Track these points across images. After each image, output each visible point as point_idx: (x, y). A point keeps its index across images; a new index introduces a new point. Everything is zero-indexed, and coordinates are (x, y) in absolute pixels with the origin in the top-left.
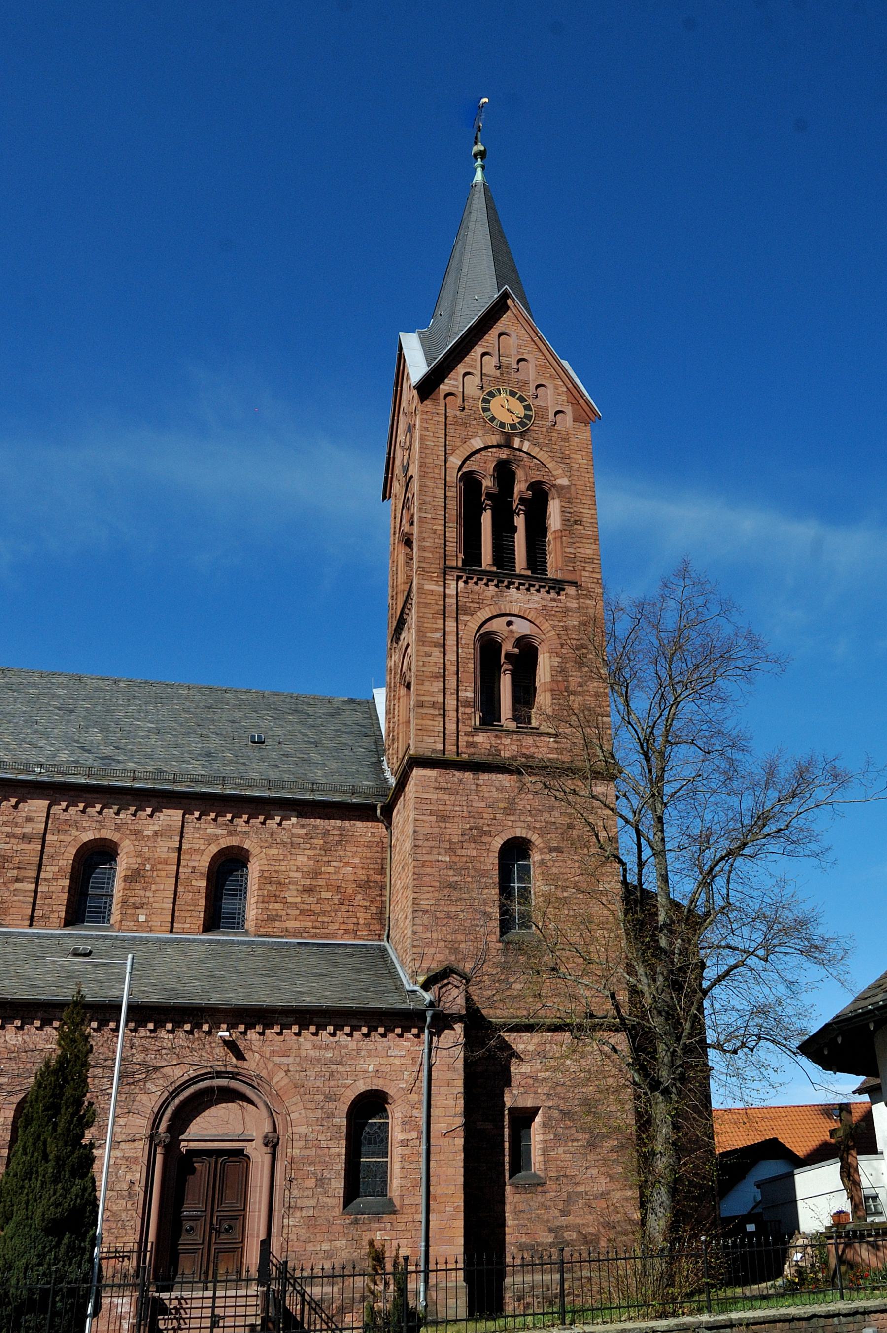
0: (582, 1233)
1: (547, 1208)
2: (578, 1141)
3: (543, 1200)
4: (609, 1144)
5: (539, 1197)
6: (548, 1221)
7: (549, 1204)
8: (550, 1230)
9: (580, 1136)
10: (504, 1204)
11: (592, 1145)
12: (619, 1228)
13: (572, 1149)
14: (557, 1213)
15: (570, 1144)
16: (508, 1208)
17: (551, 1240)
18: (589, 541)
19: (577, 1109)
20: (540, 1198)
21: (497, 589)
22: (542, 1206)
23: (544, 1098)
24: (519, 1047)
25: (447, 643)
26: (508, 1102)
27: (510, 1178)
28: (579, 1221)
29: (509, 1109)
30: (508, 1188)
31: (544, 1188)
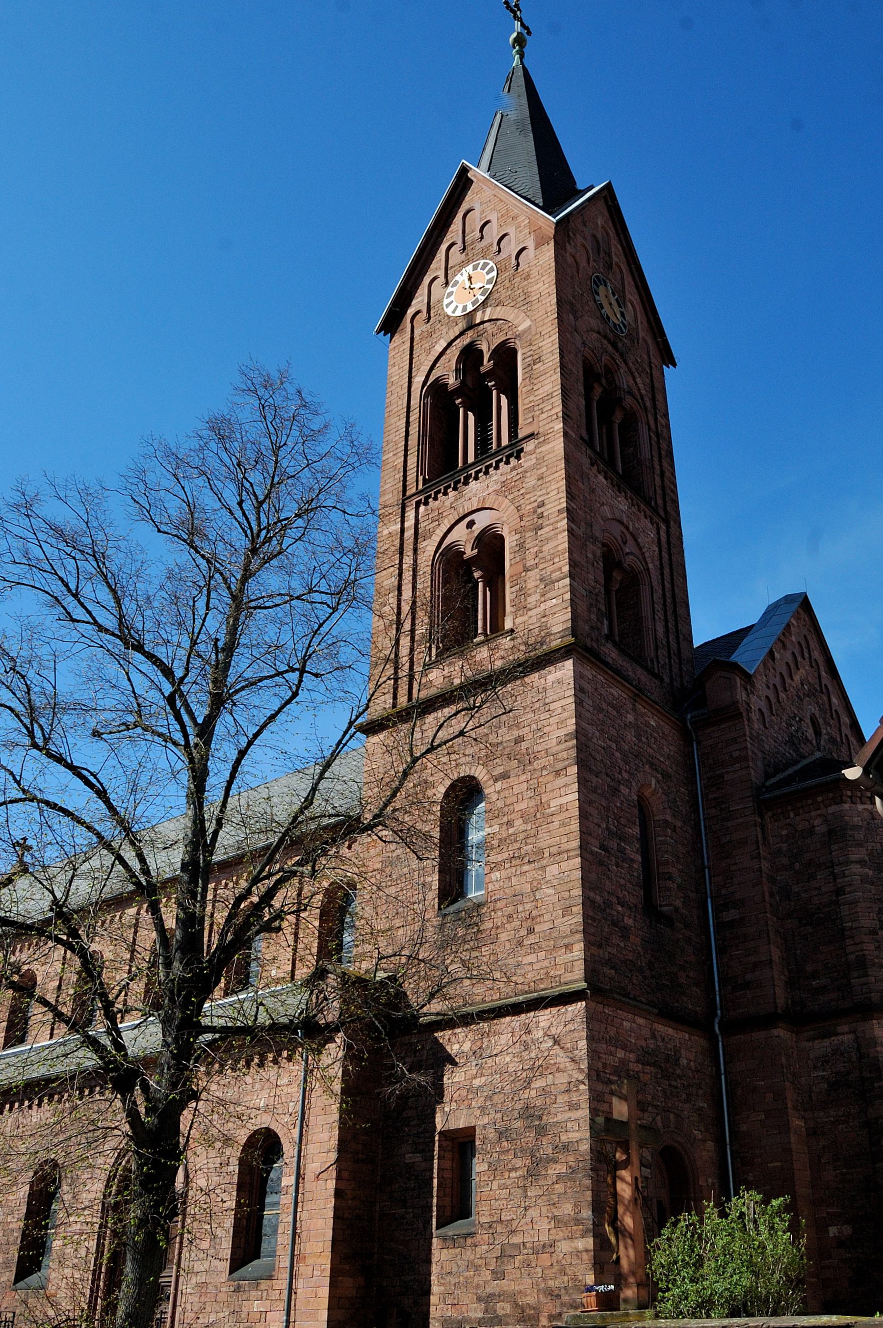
0: (517, 1305)
1: (477, 1268)
2: (515, 1169)
3: (472, 1257)
4: (555, 1170)
5: (469, 1253)
6: (477, 1287)
7: (479, 1262)
8: (479, 1299)
9: (519, 1163)
10: (429, 1262)
11: (533, 1174)
12: (566, 1298)
13: (509, 1182)
14: (487, 1275)
15: (506, 1175)
16: (435, 1269)
17: (480, 1315)
18: (548, 375)
19: (518, 1124)
20: (468, 1255)
21: (456, 493)
22: (470, 1265)
23: (478, 1113)
24: (453, 1049)
25: (70, 610)
26: (439, 1123)
27: (437, 1229)
28: (514, 1287)
29: (441, 1133)
30: (435, 1241)
31: (475, 1240)
